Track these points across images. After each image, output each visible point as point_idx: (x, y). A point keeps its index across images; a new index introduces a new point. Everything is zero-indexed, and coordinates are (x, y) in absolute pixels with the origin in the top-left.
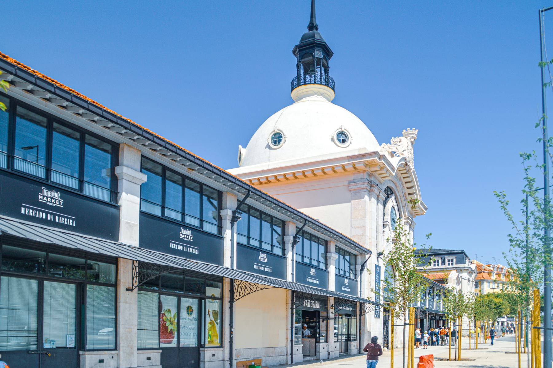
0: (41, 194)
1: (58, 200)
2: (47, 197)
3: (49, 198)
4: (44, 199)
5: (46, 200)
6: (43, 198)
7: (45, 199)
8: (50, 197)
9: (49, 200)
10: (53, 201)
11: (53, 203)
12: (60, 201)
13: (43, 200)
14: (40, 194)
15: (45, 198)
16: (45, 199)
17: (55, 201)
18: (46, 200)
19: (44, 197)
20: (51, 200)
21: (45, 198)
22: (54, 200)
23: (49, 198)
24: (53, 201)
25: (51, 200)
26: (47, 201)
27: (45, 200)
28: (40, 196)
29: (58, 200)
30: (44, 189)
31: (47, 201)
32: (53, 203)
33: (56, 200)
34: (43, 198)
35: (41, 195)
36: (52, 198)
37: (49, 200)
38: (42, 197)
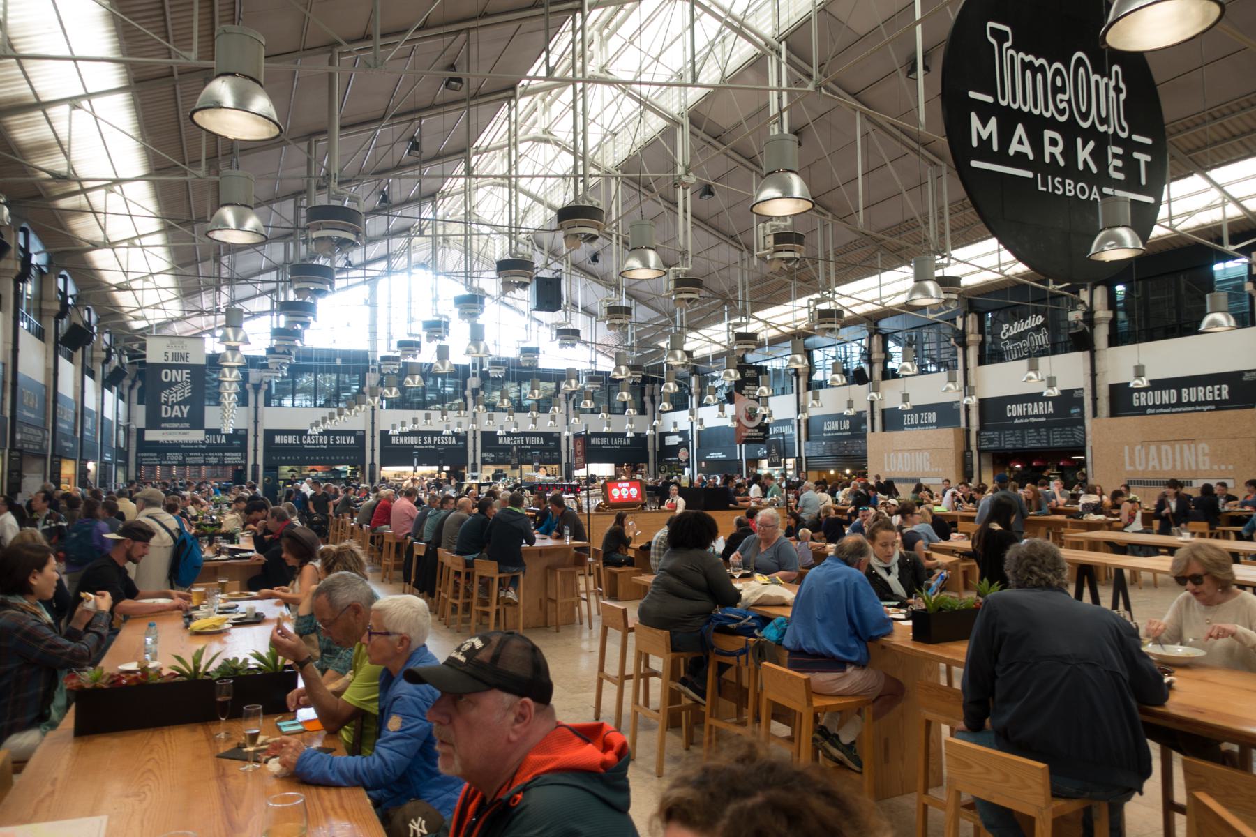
0: (990, 99)
1: (1117, 140)
2: (1036, 126)
3: (1048, 134)
4: (1014, 148)
5: (1031, 157)
6: (1006, 135)
7: (1020, 144)
8: (1052, 124)
9: (1053, 150)
10: (1084, 154)
11: (1085, 175)
12: (1129, 145)
13: (1002, 157)
14: (972, 94)
15: (1020, 130)
16: (1020, 144)
17: (1099, 155)
18: (1031, 157)
19: (1009, 119)
20: (1070, 153)
21: (1020, 130)
22: (1091, 144)
23: (1048, 134)
24: (1084, 154)
25: (1070, 153)
26: (1037, 165)
27: (1020, 161)
28: (974, 118)
29: (1117, 140)
30: (1001, 37)
31: (1037, 165)
32: (1085, 175)
33: (1103, 141)
34: (1006, 135)
35: (985, 112)
36: (1070, 131)
37: (1048, 149)
38: (993, 122)
